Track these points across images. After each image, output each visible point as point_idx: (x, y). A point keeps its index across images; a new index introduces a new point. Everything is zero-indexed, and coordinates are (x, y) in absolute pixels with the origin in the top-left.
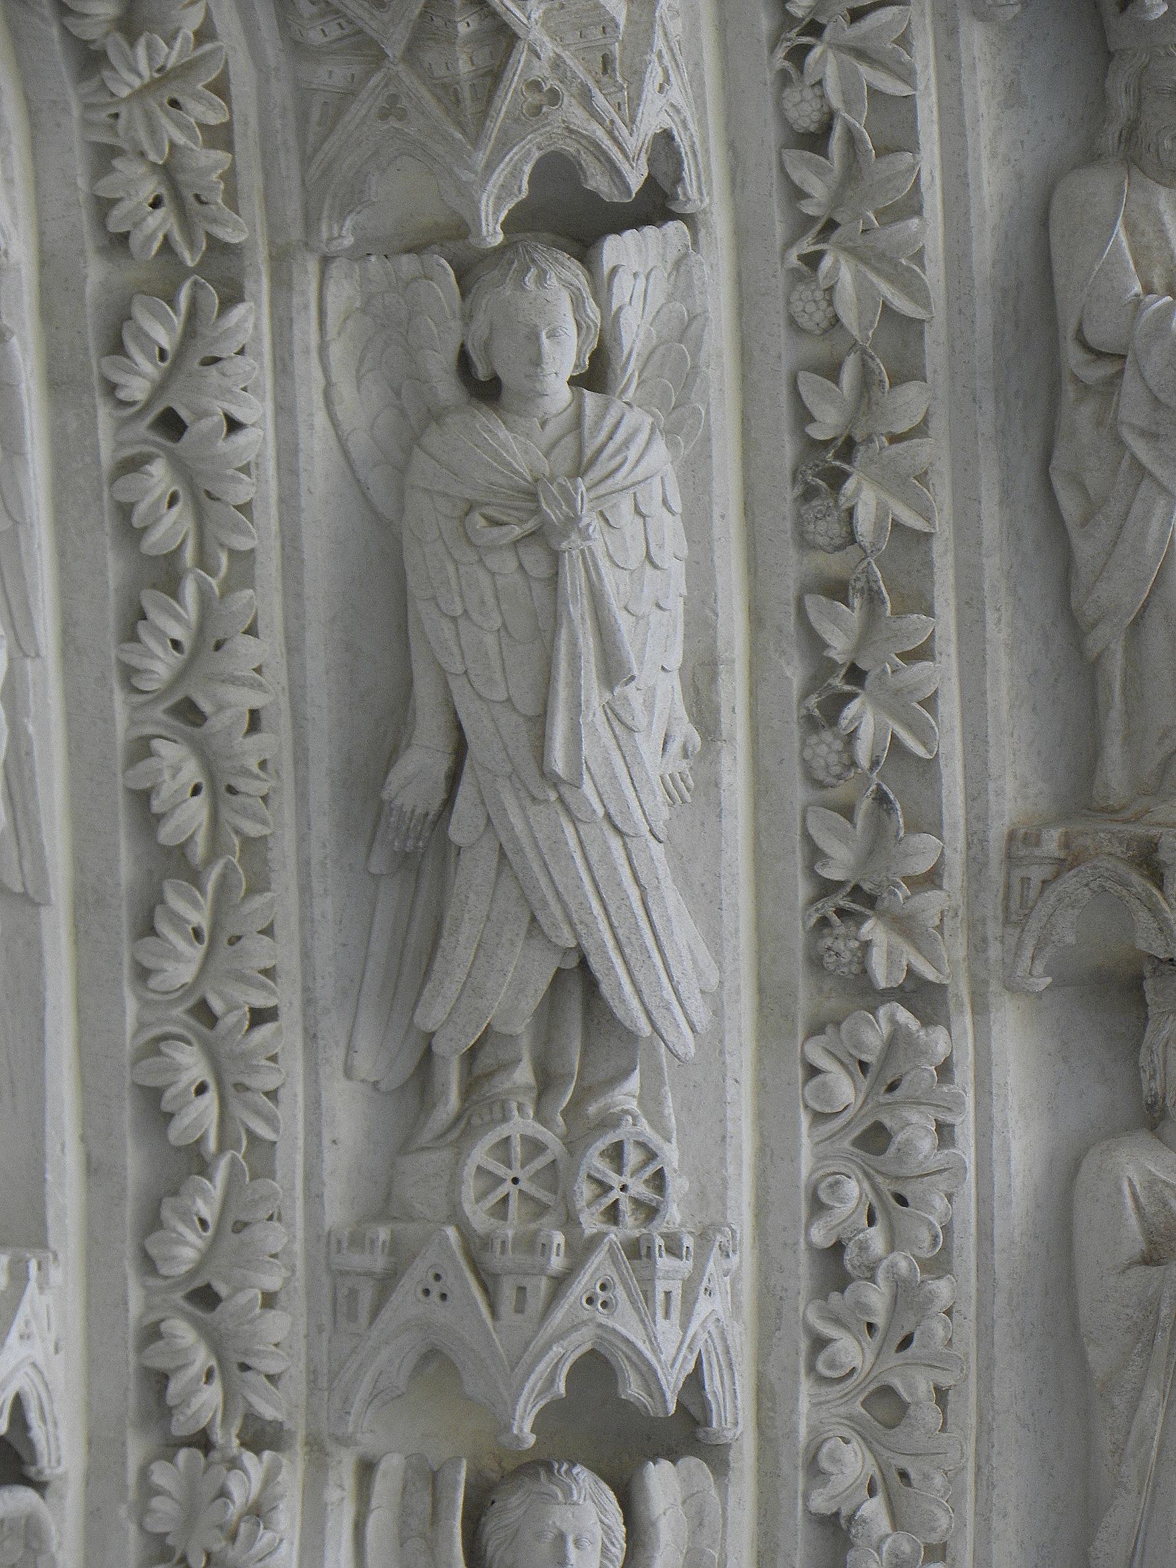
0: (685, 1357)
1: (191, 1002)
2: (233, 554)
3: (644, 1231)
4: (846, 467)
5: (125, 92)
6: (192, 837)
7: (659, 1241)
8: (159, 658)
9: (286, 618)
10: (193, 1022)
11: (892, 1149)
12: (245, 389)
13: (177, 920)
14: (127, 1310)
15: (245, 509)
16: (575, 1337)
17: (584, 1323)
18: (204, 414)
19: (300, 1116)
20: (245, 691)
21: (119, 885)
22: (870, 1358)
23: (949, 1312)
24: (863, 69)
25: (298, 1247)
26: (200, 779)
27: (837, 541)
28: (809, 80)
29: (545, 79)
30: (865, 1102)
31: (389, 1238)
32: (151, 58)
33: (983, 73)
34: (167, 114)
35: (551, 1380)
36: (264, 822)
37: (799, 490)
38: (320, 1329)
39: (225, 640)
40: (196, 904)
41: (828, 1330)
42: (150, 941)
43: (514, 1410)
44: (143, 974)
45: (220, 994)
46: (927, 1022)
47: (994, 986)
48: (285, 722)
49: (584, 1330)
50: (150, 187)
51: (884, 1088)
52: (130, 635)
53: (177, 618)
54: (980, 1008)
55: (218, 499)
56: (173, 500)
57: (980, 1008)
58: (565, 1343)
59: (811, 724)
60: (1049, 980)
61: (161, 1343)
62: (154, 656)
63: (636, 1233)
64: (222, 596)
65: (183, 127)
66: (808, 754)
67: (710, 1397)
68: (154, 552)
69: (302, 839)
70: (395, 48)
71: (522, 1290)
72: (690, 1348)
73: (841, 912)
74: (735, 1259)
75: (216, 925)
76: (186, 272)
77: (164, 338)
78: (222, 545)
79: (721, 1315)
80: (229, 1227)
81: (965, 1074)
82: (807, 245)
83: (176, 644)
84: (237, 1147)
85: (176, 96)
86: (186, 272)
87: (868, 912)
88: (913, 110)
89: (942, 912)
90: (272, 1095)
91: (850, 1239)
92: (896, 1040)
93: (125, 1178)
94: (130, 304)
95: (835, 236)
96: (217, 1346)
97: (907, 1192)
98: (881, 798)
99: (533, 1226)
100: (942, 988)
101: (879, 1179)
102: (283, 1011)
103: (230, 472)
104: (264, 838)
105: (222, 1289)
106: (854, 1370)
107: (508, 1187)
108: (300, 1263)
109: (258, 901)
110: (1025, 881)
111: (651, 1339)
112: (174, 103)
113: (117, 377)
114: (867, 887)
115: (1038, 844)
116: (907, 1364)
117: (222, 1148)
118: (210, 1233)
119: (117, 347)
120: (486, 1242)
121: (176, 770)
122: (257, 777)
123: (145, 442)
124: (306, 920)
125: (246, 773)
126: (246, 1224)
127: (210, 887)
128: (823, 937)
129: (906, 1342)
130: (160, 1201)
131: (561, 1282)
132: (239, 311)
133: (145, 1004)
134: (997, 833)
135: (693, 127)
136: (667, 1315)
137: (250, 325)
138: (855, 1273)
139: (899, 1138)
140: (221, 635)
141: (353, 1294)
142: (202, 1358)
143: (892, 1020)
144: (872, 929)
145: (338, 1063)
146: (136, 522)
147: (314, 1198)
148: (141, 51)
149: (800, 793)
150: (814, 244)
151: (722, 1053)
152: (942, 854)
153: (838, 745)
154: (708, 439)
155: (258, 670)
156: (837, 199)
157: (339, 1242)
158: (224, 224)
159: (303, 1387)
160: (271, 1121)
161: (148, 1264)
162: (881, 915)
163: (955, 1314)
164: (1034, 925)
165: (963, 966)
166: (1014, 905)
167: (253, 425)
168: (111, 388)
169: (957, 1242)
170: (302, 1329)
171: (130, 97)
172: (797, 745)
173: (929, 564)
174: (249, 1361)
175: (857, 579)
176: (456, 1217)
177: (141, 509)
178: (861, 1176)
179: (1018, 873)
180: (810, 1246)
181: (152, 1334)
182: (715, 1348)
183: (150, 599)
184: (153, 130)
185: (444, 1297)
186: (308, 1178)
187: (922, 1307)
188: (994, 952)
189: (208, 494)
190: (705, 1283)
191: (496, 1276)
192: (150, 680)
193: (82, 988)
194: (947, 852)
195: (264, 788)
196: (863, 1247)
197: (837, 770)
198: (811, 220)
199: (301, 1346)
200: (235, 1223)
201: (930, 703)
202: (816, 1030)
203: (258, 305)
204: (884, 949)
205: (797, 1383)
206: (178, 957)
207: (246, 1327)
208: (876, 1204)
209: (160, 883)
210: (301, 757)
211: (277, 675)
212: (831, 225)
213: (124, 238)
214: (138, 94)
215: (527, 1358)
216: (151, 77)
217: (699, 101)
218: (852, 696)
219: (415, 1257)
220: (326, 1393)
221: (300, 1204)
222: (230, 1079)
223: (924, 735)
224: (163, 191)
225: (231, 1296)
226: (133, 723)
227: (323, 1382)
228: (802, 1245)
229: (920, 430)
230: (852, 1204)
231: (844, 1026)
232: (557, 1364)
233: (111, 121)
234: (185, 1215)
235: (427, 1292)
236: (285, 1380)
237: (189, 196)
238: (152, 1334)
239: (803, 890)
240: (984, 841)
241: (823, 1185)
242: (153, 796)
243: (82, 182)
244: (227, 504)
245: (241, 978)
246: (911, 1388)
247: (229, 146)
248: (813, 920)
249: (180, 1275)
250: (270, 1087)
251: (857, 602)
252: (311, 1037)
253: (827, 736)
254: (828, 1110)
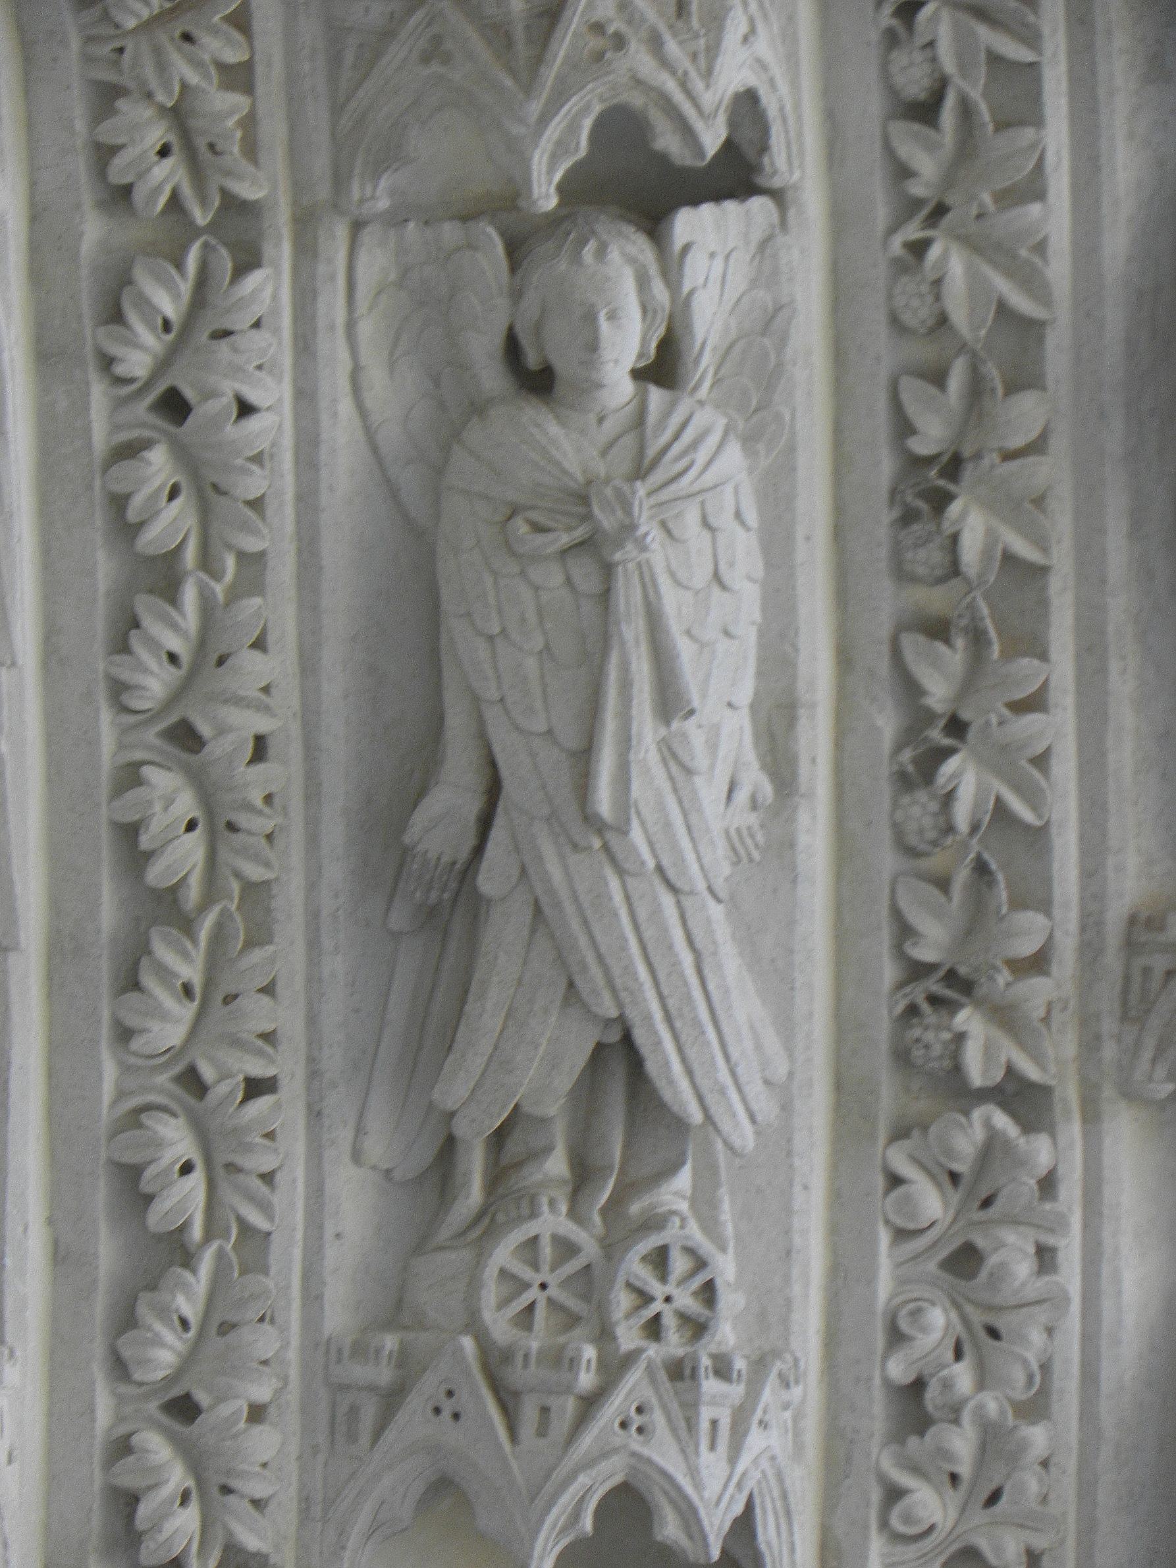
0: (732, 1498)
1: (178, 1069)
2: (242, 556)
3: (689, 1349)
4: (951, 487)
5: (131, 23)
6: (185, 878)
7: (705, 1362)
8: (152, 673)
9: (300, 635)
10: (179, 1091)
11: (984, 1274)
12: (259, 367)
13: (164, 973)
14: (93, 1420)
15: (256, 504)
16: (605, 1466)
17: (615, 1450)
18: (211, 394)
19: (300, 1204)
20: (248, 713)
21: (98, 931)
22: (953, 1515)
23: (1045, 1464)
24: (985, 34)
25: (292, 1355)
26: (195, 813)
27: (939, 572)
28: (920, 40)
29: (610, 21)
30: (955, 1220)
31: (396, 1348)
33: (1120, 40)
34: (179, 49)
35: (576, 1516)
36: (267, 865)
37: (896, 513)
38: (315, 1450)
39: (229, 655)
40: (185, 956)
41: (904, 1479)
42: (133, 996)
43: (532, 1548)
44: (124, 1034)
45: (212, 1060)
46: (1028, 1128)
47: (1108, 1091)
48: (295, 751)
49: (615, 1459)
50: (157, 133)
51: (977, 1204)
52: (121, 646)
53: (174, 627)
54: (1091, 1116)
55: (225, 493)
56: (174, 493)
57: (1091, 1116)
58: (594, 1472)
59: (905, 782)
60: (1170, 1087)
61: (131, 1459)
62: (146, 670)
63: (680, 1352)
64: (227, 605)
65: (197, 64)
66: (899, 815)
67: (763, 1547)
68: (151, 551)
69: (312, 887)
71: (545, 1410)
72: (739, 1486)
73: (935, 1000)
74: (797, 1392)
75: (209, 982)
76: (194, 232)
77: (169, 306)
78: (229, 546)
79: (777, 1451)
80: (213, 1330)
81: (1071, 1191)
82: (913, 231)
83: (173, 658)
84: (227, 1237)
85: (189, 28)
86: (194, 232)
87: (964, 999)
88: (1038, 80)
89: (1050, 1004)
90: (268, 1178)
91: (932, 1375)
92: (992, 1148)
93: (97, 1267)
94: (130, 268)
95: (947, 221)
96: (196, 1467)
97: (1001, 1323)
98: (981, 868)
99: (561, 1339)
100: (1045, 1091)
101: (969, 1309)
102: (283, 1083)
103: (239, 462)
104: (266, 883)
105: (202, 1398)
106: (932, 1528)
107: (533, 1293)
108: (294, 1373)
109: (257, 955)
110: (1147, 971)
111: (693, 1472)
112: (187, 37)
113: (114, 350)
114: (963, 970)
115: (1162, 928)
116: (997, 1523)
117: (208, 1237)
118: (192, 1333)
119: (115, 316)
120: (507, 1356)
121: (169, 802)
122: (260, 813)
123: (144, 425)
124: (313, 980)
125: (249, 807)
126: (233, 1326)
127: (204, 935)
128: (911, 1027)
129: (994, 1498)
130: (136, 1299)
131: (591, 1403)
132: (254, 279)
133: (126, 1069)
134: (1115, 915)
135: (784, 88)
136: (713, 1447)
137: (267, 293)
138: (937, 1415)
139: (993, 1260)
140: (223, 649)
141: (354, 1411)
142: (177, 1477)
143: (988, 1124)
144: (967, 1019)
145: (346, 1145)
146: (132, 515)
147: (312, 1298)
149: (888, 861)
150: (924, 229)
151: (789, 1154)
152: (1050, 938)
153: (934, 806)
154: (791, 449)
155: (266, 690)
156: (949, 180)
157: (340, 1351)
158: (240, 177)
159: (292, 1516)
160: (266, 1208)
161: (120, 1368)
162: (979, 1004)
163: (1053, 1469)
164: (1155, 1022)
165: (1072, 1070)
166: (1134, 998)
167: (268, 409)
168: (107, 362)
169: (1057, 1383)
170: (293, 1448)
171: (135, 31)
172: (886, 805)
173: (1043, 603)
174: (234, 1483)
175: (960, 616)
176: (474, 1325)
177: (137, 501)
178: (948, 1304)
179: (1140, 962)
180: (887, 1382)
181: (122, 1448)
182: (771, 1492)
183: (144, 605)
184: (162, 67)
185: (456, 1416)
186: (306, 1276)
187: (1014, 1456)
188: (1109, 1051)
189: (215, 487)
190: (759, 1413)
191: (517, 1394)
192: (142, 697)
193: (55, 1049)
194: (1058, 934)
195: (268, 825)
196: (947, 1385)
197: (931, 835)
198: (918, 203)
199: (292, 1469)
200: (221, 1325)
201: (1041, 761)
202: (900, 1133)
203: (278, 273)
204: (981, 1041)
205: (866, 1538)
206: (164, 1016)
207: (228, 1443)
208: (964, 1337)
209: (146, 932)
210: (313, 793)
211: (288, 697)
212: (940, 211)
213: (126, 191)
214: (147, 26)
215: (549, 1488)
216: (161, 7)
217: (792, 61)
218: (948, 753)
219: (424, 1370)
220: (319, 1526)
221: (296, 1305)
222: (221, 1158)
223: (1033, 798)
224: (172, 138)
225: (212, 1407)
226: (121, 747)
227: (317, 1510)
228: (877, 1381)
229: (1037, 447)
230: (936, 1335)
231: (933, 1130)
232: (583, 1497)
233: (115, 56)
234: (163, 1312)
235: (437, 1411)
236: (272, 1507)
237: (201, 143)
238: (122, 1448)
239: (889, 972)
240: (1100, 924)
241: (904, 1312)
242: (142, 831)
243: (80, 125)
244: (236, 499)
245: (236, 1043)
246: (998, 1549)
247: (248, 88)
248: (900, 1007)
249: (154, 1383)
250: (266, 1168)
251: (960, 642)
252: (315, 1114)
253: (922, 795)
254: (911, 1226)
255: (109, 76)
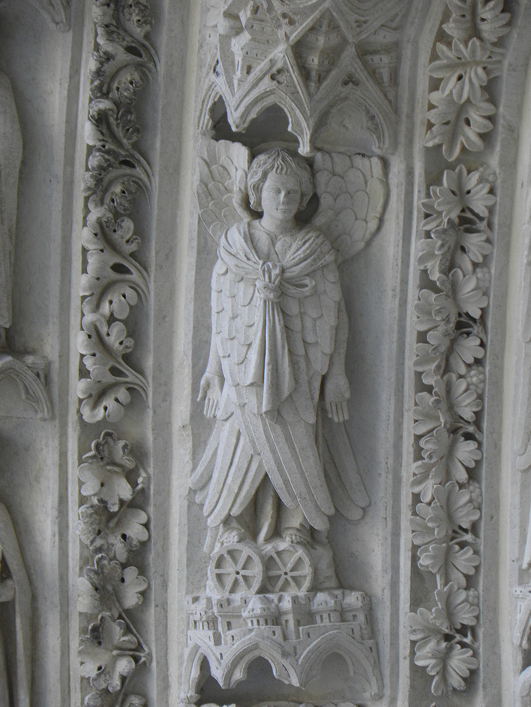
32: (462, 89)
50: (484, 27)
65: (458, 50)
70: (350, 51)
148: (465, 96)
184: (473, 52)
237: (468, 17)
255: (496, 50)
